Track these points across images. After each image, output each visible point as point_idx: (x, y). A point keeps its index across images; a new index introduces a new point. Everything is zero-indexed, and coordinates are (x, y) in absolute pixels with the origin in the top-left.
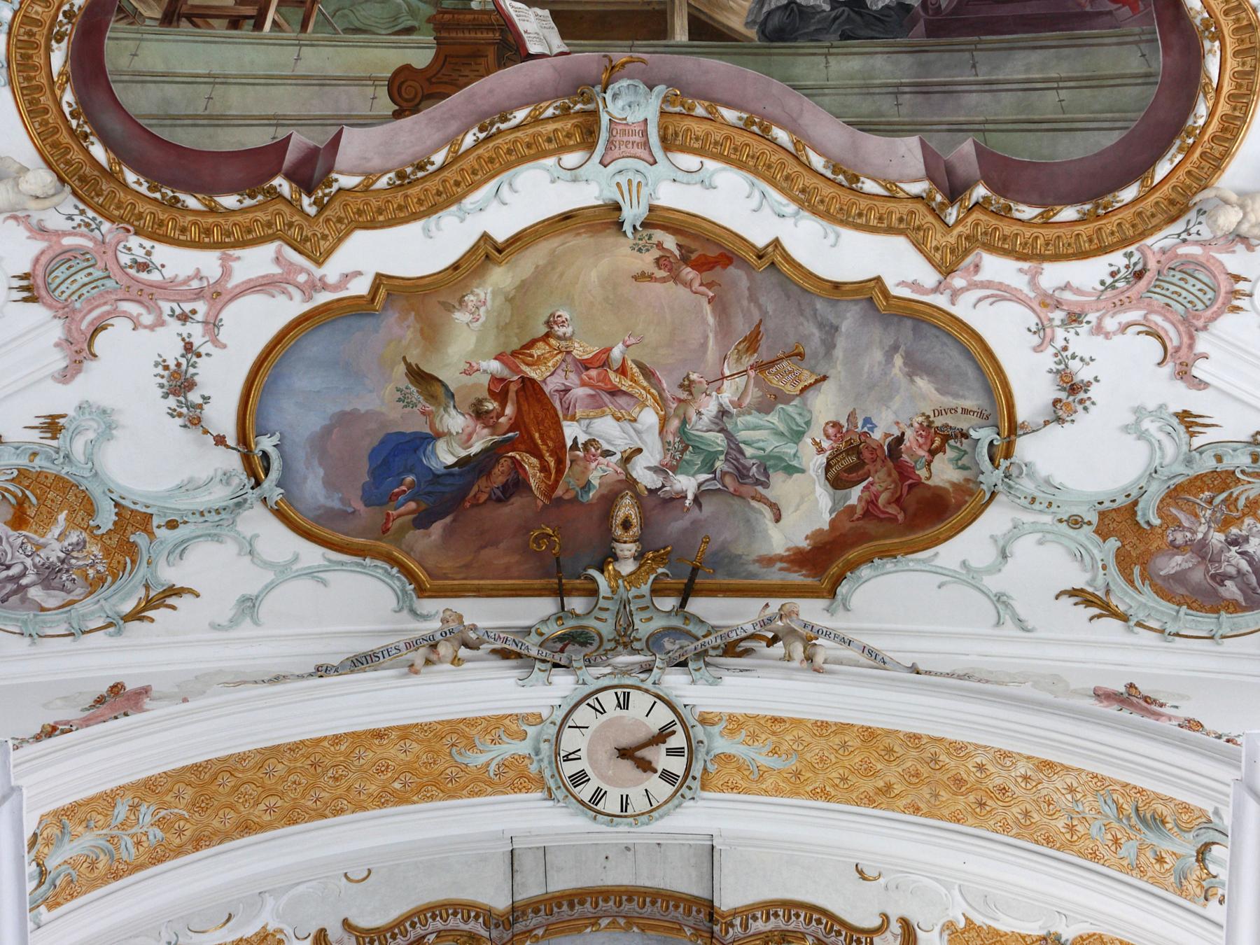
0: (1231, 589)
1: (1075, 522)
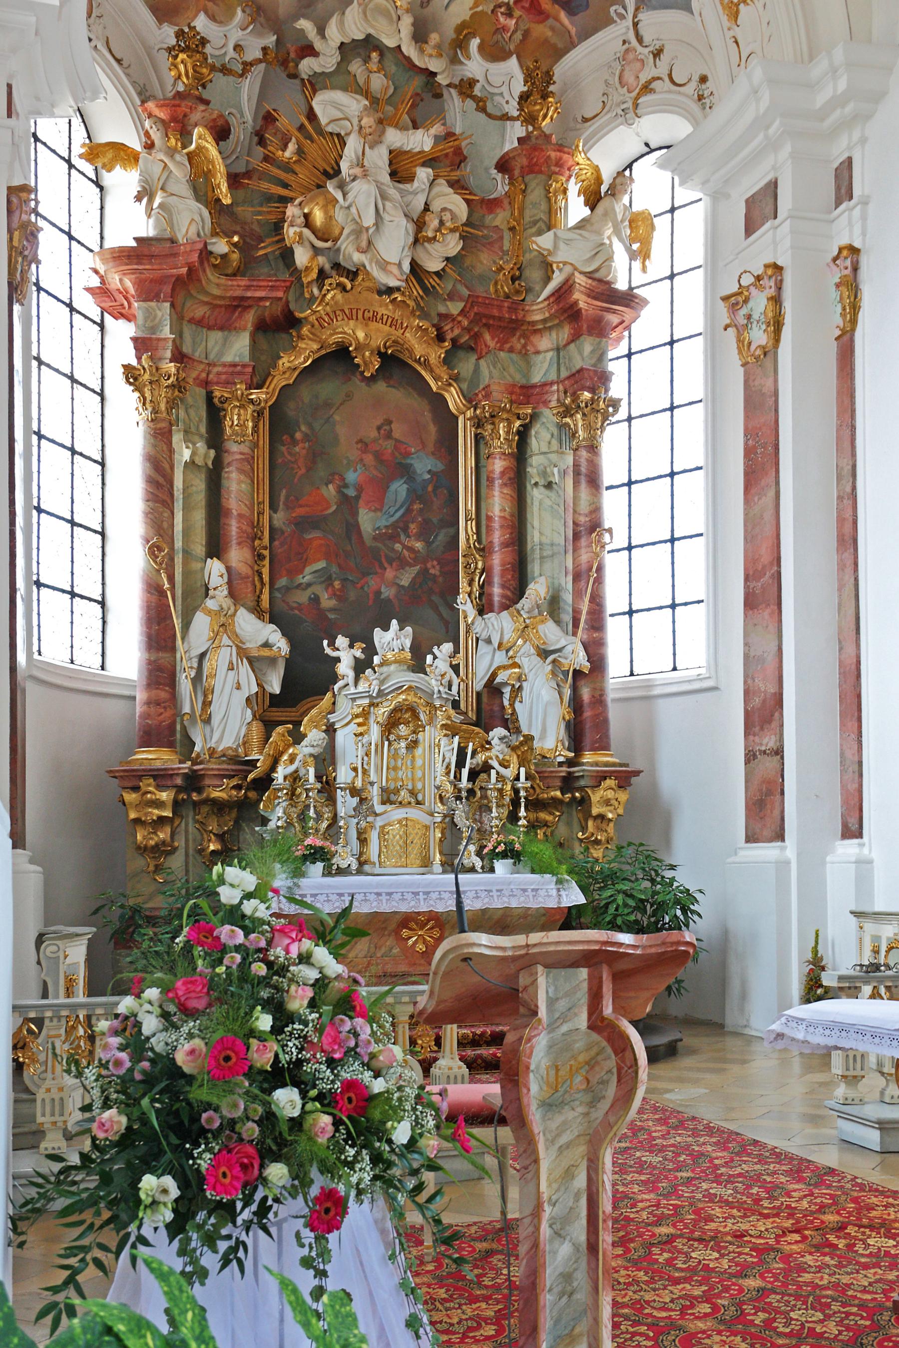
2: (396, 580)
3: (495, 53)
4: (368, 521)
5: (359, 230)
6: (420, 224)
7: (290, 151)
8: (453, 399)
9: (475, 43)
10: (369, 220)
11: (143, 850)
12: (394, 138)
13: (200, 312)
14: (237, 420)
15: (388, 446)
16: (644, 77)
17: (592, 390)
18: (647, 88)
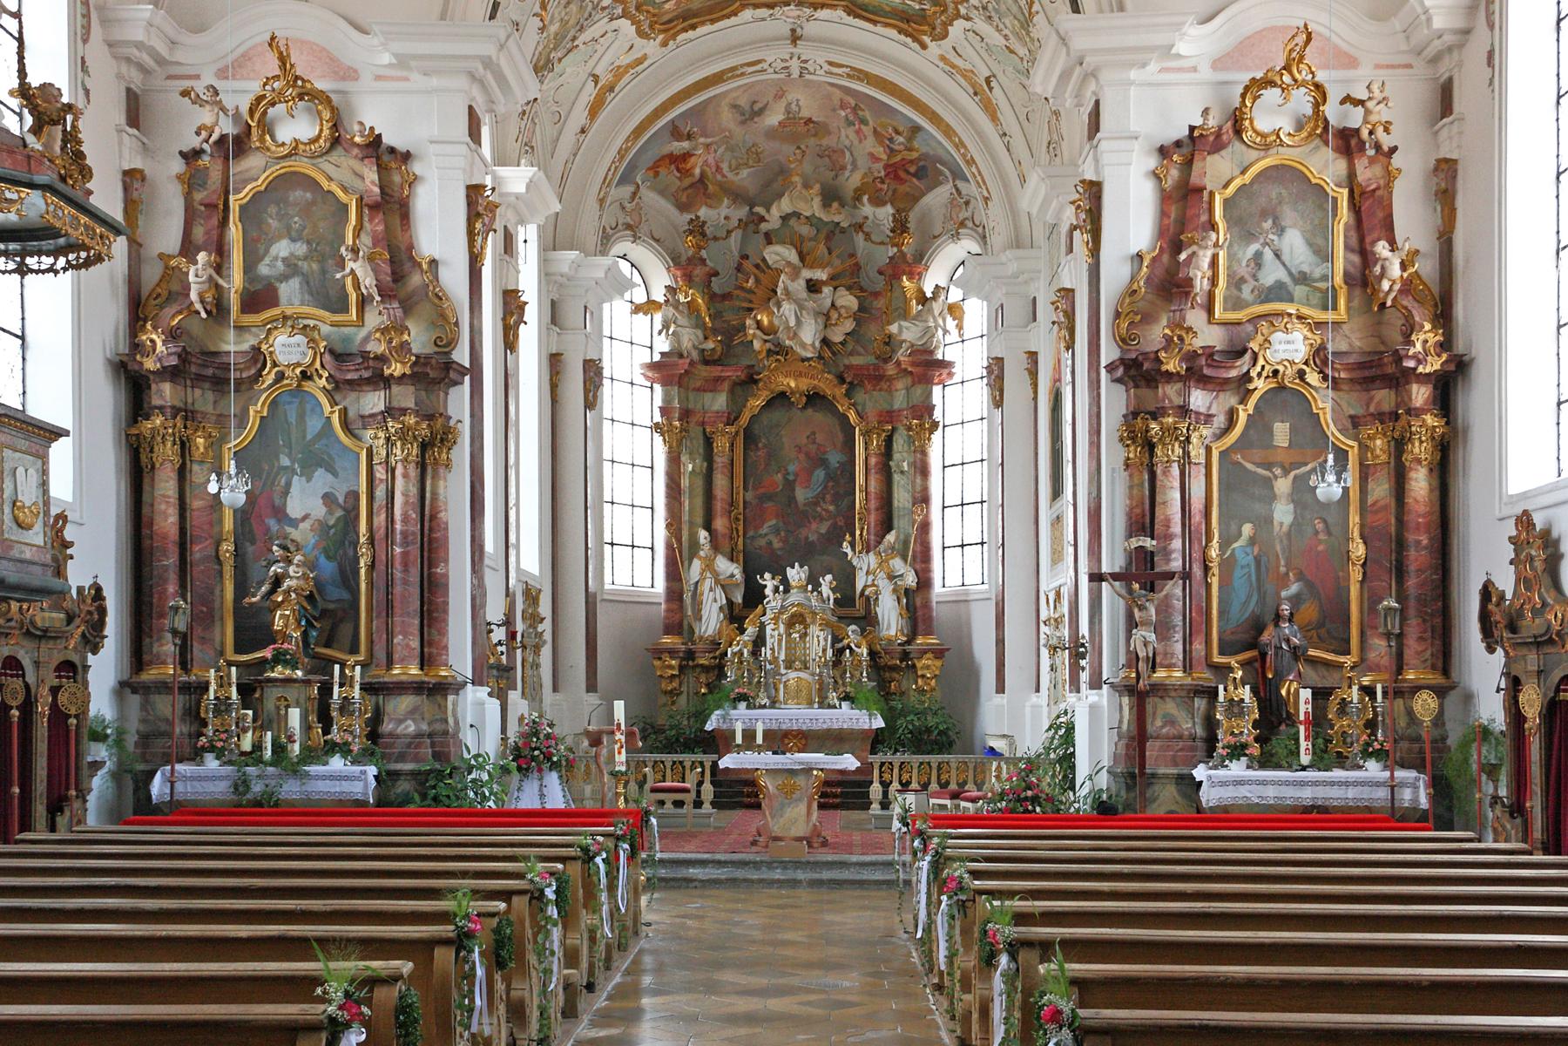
2: (816, 531)
3: (878, 202)
4: (801, 495)
5: (788, 328)
6: (827, 316)
9: (865, 198)
10: (792, 323)
11: (665, 692)
12: (807, 274)
13: (698, 384)
14: (721, 444)
15: (813, 448)
16: (961, 217)
17: (920, 418)
18: (962, 224)
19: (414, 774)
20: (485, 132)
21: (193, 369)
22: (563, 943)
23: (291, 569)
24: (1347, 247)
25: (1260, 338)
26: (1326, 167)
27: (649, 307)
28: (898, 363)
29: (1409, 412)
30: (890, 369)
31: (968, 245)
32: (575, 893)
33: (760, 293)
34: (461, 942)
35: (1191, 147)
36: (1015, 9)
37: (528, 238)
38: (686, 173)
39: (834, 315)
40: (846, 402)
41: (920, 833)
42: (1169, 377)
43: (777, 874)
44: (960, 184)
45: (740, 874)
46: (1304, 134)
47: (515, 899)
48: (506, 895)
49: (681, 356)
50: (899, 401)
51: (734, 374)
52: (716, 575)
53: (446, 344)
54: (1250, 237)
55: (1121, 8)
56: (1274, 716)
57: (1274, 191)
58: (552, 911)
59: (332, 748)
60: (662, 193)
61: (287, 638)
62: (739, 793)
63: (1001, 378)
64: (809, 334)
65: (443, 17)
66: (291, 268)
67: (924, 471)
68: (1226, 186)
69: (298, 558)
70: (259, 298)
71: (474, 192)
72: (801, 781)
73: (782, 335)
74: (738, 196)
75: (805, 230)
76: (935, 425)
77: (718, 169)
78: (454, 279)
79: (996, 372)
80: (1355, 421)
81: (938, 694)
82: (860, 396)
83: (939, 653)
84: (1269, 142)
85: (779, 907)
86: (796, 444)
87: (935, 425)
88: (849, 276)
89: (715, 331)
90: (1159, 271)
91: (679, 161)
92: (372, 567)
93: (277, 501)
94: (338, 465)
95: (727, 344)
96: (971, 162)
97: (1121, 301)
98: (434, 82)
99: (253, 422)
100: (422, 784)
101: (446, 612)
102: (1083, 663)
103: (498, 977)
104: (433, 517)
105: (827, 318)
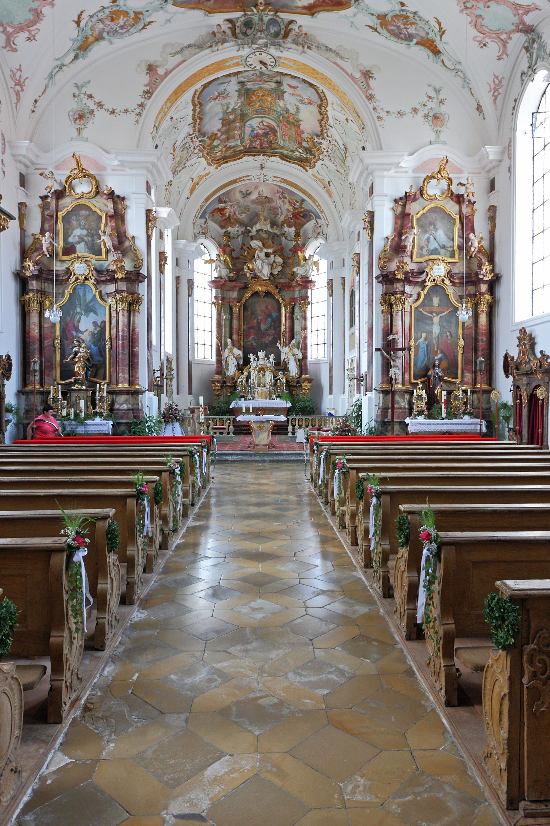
0: (402, 36)
1: (372, 14)
2: (268, 339)
3: (290, 226)
4: (263, 327)
5: (259, 269)
6: (272, 265)
7: (246, 253)
8: (280, 300)
10: (260, 267)
12: (265, 250)
14: (235, 309)
17: (304, 300)
18: (319, 234)
19: (126, 424)
20: (153, 191)
21: (44, 276)
22: (182, 490)
23: (81, 350)
24: (459, 236)
25: (429, 267)
26: (452, 208)
27: (211, 261)
28: (297, 281)
29: (480, 294)
30: (294, 284)
31: (320, 241)
32: (187, 469)
33: (249, 257)
34: (139, 496)
35: (406, 199)
36: (340, 156)
37: (168, 234)
38: (223, 215)
39: (275, 265)
40: (278, 295)
41: (316, 444)
42: (398, 280)
43: (258, 458)
44: (318, 220)
45: (244, 458)
46: (444, 196)
47: (163, 474)
48: (159, 473)
49: (222, 278)
50: (297, 295)
51: (240, 284)
52: (233, 354)
53: (137, 267)
54: (426, 232)
55: (381, 149)
56: (432, 400)
57: (434, 216)
58: (179, 479)
59: (96, 414)
60: (215, 222)
61: (79, 374)
62: (244, 429)
63: (332, 286)
64: (266, 272)
65: (137, 147)
66: (81, 239)
67: (305, 319)
68: (417, 214)
69: (83, 345)
70: (69, 250)
71: (148, 212)
72: (265, 425)
73: (257, 272)
74: (241, 223)
75: (265, 235)
76: (309, 303)
77: (235, 214)
78: (141, 244)
79: (330, 285)
80: (461, 297)
81: (309, 395)
82: (283, 293)
83: (310, 381)
84: (432, 199)
85: (259, 470)
86: (260, 310)
87: (309, 303)
88: (279, 251)
89: (233, 270)
90: (394, 243)
91: (221, 211)
92: (111, 348)
93: (76, 325)
94: (98, 311)
95: (238, 275)
96: (322, 212)
97: (381, 254)
98: (134, 171)
99: (67, 296)
100: (129, 427)
101: (138, 365)
102: (362, 383)
103: (156, 507)
104: (133, 330)
105: (272, 266)
